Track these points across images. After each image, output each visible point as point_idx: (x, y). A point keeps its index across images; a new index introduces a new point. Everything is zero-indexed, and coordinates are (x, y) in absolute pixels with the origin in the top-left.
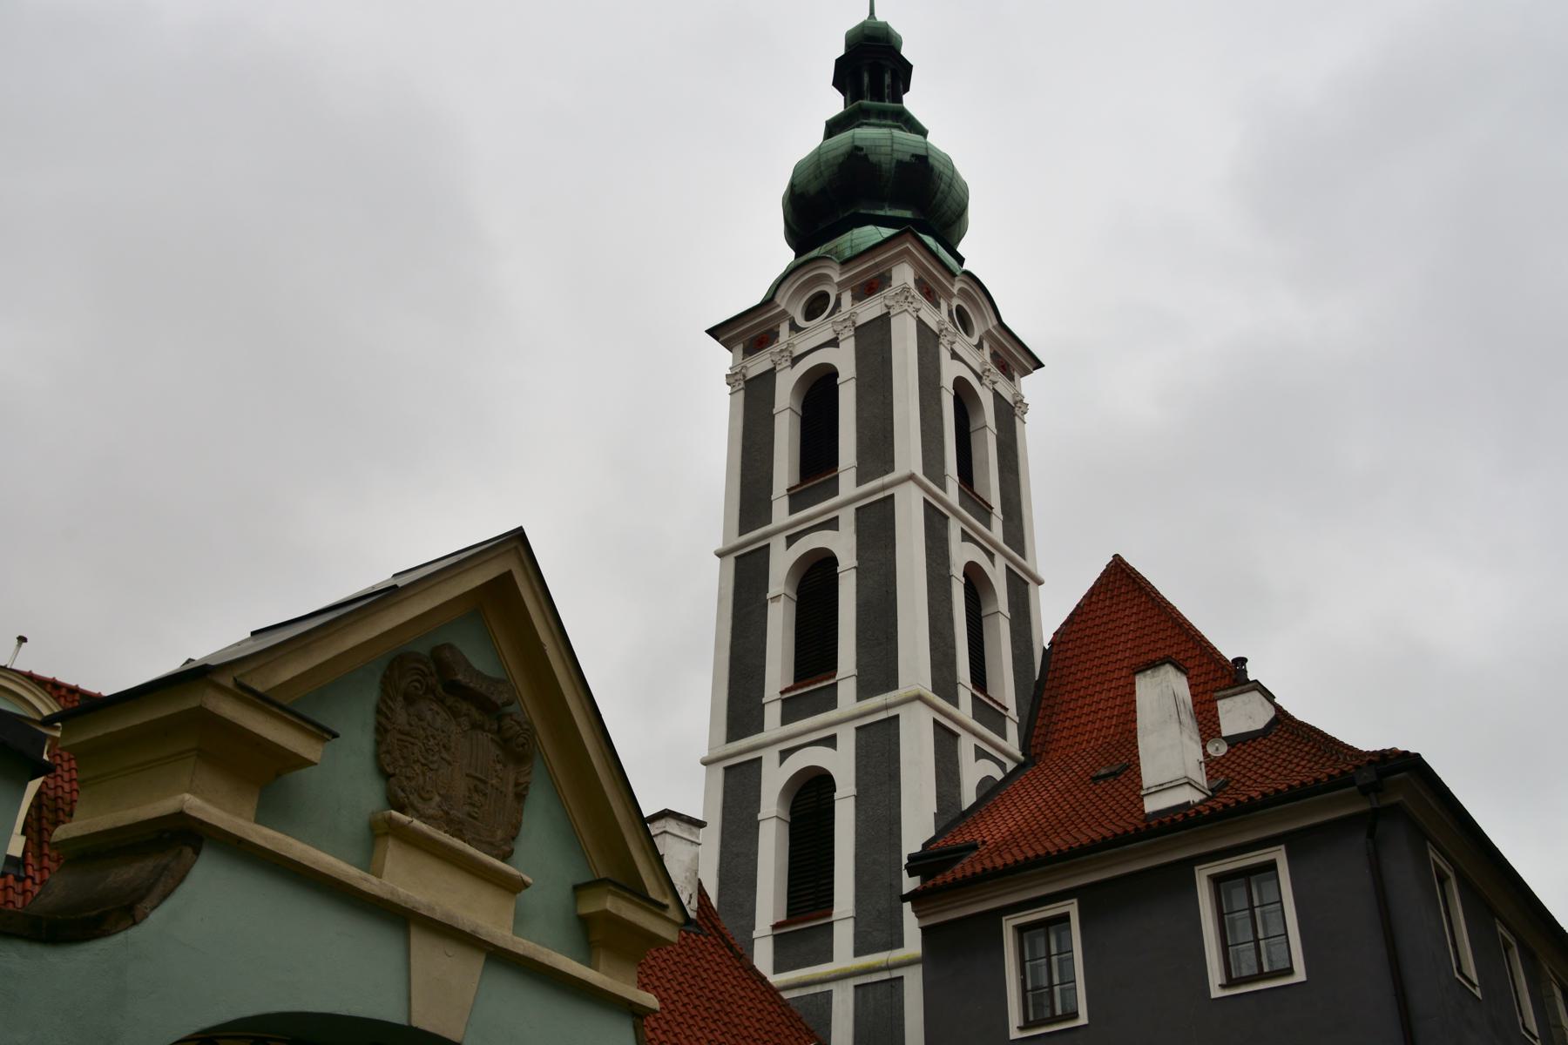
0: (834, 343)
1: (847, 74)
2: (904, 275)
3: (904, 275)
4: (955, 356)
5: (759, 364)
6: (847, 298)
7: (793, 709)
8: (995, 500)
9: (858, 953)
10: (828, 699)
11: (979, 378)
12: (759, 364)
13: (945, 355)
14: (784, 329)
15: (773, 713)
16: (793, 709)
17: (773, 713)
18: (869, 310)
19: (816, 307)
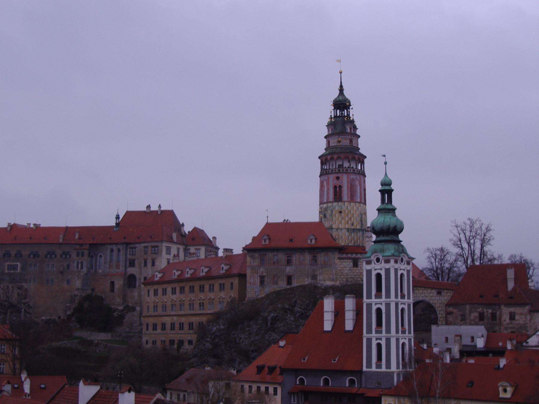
0: (381, 269)
1: (382, 192)
2: (392, 261)
3: (392, 261)
4: (401, 269)
5: (369, 267)
6: (383, 261)
7: (377, 332)
8: (406, 293)
9: (386, 368)
10: (382, 333)
11: (404, 270)
12: (369, 267)
13: (399, 271)
14: (373, 262)
15: (374, 331)
16: (377, 332)
17: (374, 331)
18: (387, 266)
19: (378, 260)
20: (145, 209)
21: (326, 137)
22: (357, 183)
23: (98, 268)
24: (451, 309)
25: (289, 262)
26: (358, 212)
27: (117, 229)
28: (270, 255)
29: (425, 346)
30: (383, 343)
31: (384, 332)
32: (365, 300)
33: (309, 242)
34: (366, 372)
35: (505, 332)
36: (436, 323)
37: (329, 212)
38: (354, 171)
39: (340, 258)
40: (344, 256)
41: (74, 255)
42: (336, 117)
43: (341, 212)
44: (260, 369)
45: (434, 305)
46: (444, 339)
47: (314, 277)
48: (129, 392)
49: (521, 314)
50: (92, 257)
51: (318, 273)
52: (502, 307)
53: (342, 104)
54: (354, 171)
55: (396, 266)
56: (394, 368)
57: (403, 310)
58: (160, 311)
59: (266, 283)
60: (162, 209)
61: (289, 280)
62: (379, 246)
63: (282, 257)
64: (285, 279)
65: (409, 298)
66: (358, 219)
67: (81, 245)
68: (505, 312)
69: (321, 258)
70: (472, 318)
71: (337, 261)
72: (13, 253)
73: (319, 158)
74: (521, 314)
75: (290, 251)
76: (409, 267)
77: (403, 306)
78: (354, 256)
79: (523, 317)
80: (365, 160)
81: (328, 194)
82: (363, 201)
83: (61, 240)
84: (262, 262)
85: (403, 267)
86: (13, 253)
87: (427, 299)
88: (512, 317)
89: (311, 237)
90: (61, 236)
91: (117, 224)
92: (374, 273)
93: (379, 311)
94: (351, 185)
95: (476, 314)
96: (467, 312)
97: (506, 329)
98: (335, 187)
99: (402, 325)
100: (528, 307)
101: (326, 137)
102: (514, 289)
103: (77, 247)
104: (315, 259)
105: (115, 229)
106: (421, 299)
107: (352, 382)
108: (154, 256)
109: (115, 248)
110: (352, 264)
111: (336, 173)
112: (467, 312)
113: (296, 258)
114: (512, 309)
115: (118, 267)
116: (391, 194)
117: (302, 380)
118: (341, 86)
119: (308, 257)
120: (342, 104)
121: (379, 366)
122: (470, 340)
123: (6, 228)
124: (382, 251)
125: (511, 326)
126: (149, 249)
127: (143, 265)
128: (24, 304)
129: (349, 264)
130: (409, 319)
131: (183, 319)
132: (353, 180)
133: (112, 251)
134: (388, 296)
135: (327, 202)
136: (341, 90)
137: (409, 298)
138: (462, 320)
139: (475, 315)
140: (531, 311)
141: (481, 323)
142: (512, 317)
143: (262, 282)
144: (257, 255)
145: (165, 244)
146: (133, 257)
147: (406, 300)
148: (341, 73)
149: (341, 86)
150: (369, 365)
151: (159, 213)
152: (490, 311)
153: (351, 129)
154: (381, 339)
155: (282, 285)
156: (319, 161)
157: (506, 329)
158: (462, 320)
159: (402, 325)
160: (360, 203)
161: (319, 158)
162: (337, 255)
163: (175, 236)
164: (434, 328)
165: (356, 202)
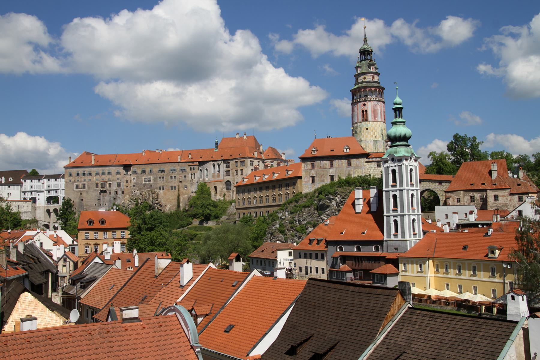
21: (355, 76)
22: (378, 107)
23: (205, 177)
24: (449, 194)
25: (332, 165)
26: (380, 129)
27: (217, 150)
29: (430, 221)
30: (399, 219)
31: (399, 211)
32: (384, 189)
33: (345, 150)
34: (386, 241)
35: (490, 209)
36: (438, 204)
37: (359, 129)
39: (367, 162)
40: (370, 160)
41: (188, 169)
42: (361, 61)
43: (367, 129)
44: (311, 242)
45: (437, 192)
46: (445, 217)
47: (349, 175)
48: (188, 263)
49: (503, 196)
50: (201, 170)
51: (352, 173)
52: (488, 191)
56: (407, 237)
57: (412, 195)
58: (247, 205)
59: (315, 181)
60: (247, 135)
61: (332, 177)
62: (393, 149)
64: (329, 178)
65: (417, 186)
66: (380, 133)
67: (193, 162)
68: (491, 195)
69: (354, 162)
70: (465, 200)
72: (147, 171)
73: (351, 91)
74: (503, 196)
75: (331, 158)
76: (417, 164)
77: (412, 192)
79: (505, 198)
81: (358, 116)
82: (383, 120)
83: (179, 160)
84: (313, 166)
86: (147, 171)
87: (431, 188)
88: (496, 198)
89: (347, 148)
90: (179, 157)
91: (217, 147)
92: (390, 169)
93: (395, 197)
94: (374, 109)
95: (469, 197)
96: (461, 196)
97: (491, 207)
98: (363, 111)
99: (412, 206)
100: (509, 190)
101: (355, 76)
102: (498, 178)
103: (191, 164)
104: (349, 164)
105: (215, 151)
106: (427, 188)
107: (377, 249)
108: (242, 168)
109: (216, 163)
110: (376, 165)
111: (363, 101)
112: (461, 196)
113: (336, 162)
114: (496, 193)
115: (218, 176)
116: (401, 110)
117: (341, 249)
119: (345, 162)
121: (396, 235)
122: (464, 216)
124: (396, 152)
125: (495, 205)
126: (239, 163)
127: (235, 174)
128: (157, 204)
130: (417, 201)
131: (262, 209)
132: (375, 105)
133: (214, 165)
134: (401, 184)
135: (357, 123)
136: (365, 41)
137: (417, 186)
138: (458, 202)
139: (467, 197)
140: (511, 194)
141: (472, 204)
142: (496, 198)
143: (313, 181)
145: (249, 160)
146: (228, 169)
147: (414, 188)
148: (365, 28)
150: (389, 235)
152: (479, 195)
154: (396, 216)
155: (328, 181)
156: (351, 93)
157: (491, 207)
158: (458, 202)
159: (412, 206)
160: (381, 122)
161: (351, 91)
162: (365, 160)
163: (256, 154)
164: (437, 208)
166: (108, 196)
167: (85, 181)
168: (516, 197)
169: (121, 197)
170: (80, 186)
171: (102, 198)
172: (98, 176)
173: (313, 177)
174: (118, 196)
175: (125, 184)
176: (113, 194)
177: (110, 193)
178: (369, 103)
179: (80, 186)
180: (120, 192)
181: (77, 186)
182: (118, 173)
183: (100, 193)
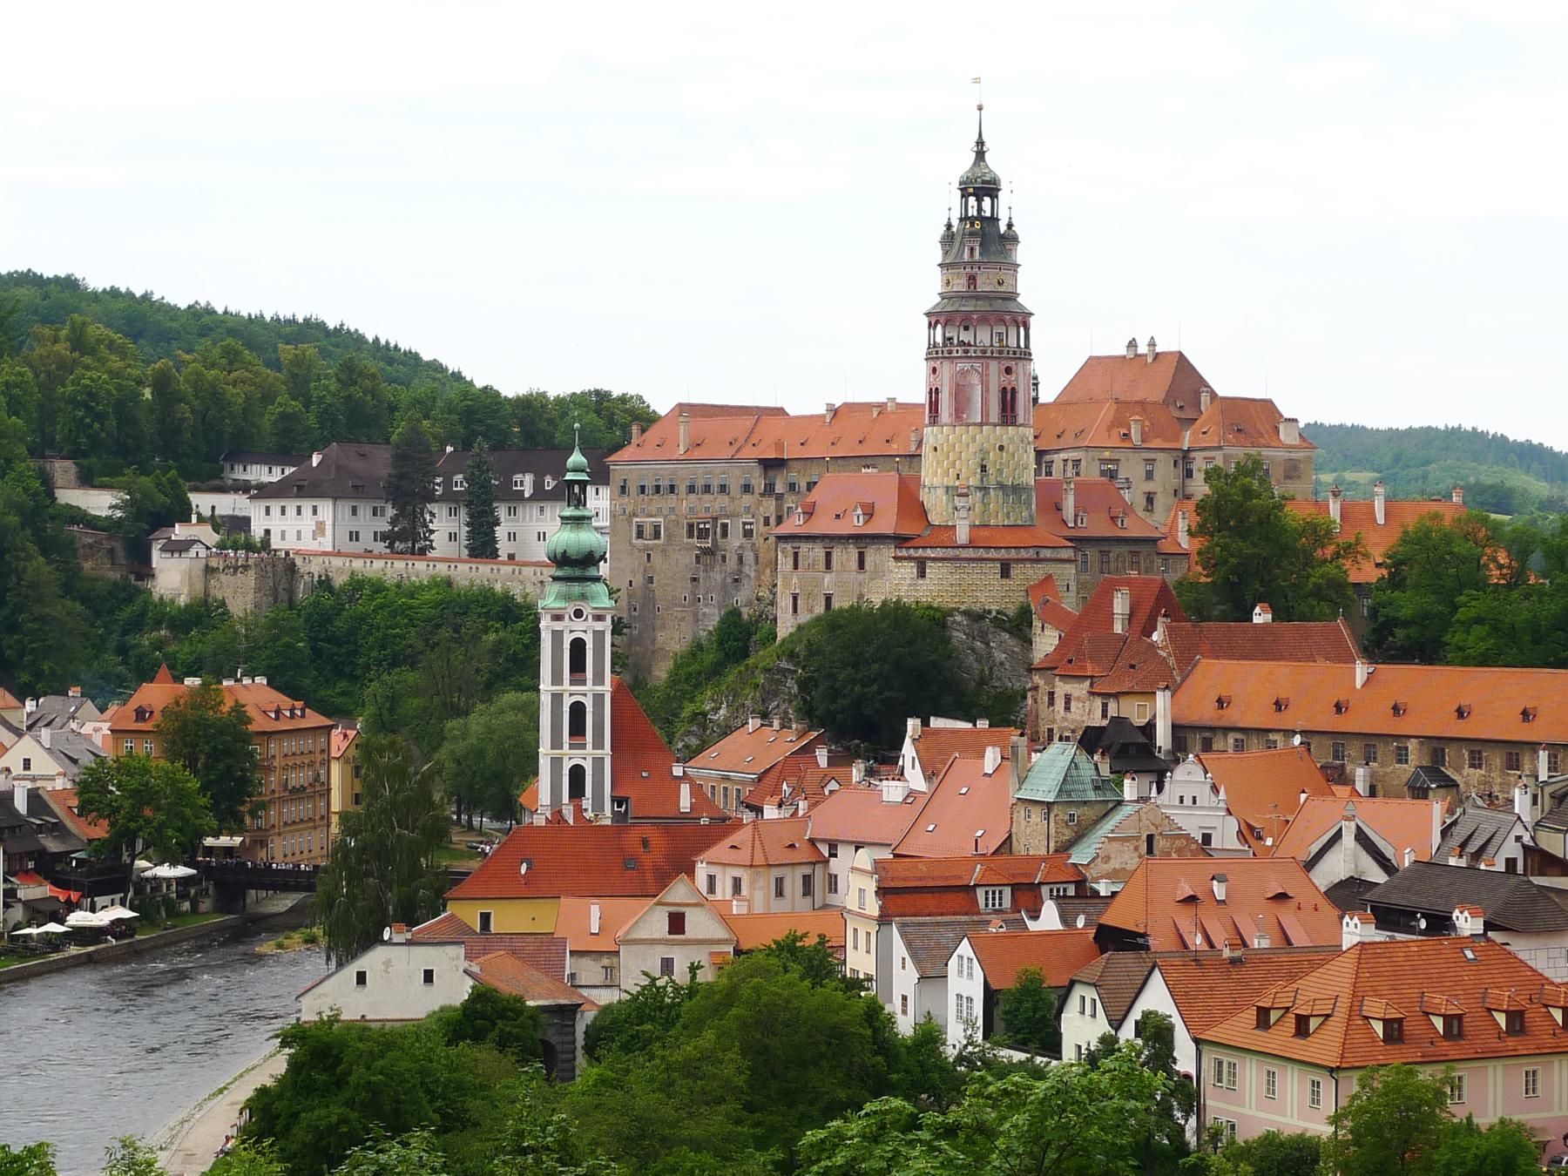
20: (1122, 351)
28: (804, 548)
38: (966, 352)
40: (904, 553)
47: (861, 596)
49: (1078, 699)
53: (981, 187)
54: (966, 352)
55: (558, 626)
60: (1158, 350)
63: (816, 552)
66: (974, 464)
71: (892, 563)
78: (920, 553)
80: (1032, 319)
85: (579, 625)
118: (980, 143)
120: (981, 187)
123: (823, 416)
129: (910, 569)
132: (963, 373)
144: (789, 547)
148: (980, 108)
149: (980, 143)
151: (1150, 360)
153: (972, 249)
160: (981, 424)
165: (968, 425)
166: (717, 568)
167: (659, 512)
168: (1098, 702)
169: (753, 575)
170: (648, 531)
171: (702, 575)
172: (693, 496)
173: (795, 598)
174: (746, 569)
175: (762, 528)
176: (732, 563)
177: (724, 557)
178: (946, 364)
179: (648, 531)
180: (749, 557)
181: (640, 535)
182: (747, 488)
183: (697, 557)
